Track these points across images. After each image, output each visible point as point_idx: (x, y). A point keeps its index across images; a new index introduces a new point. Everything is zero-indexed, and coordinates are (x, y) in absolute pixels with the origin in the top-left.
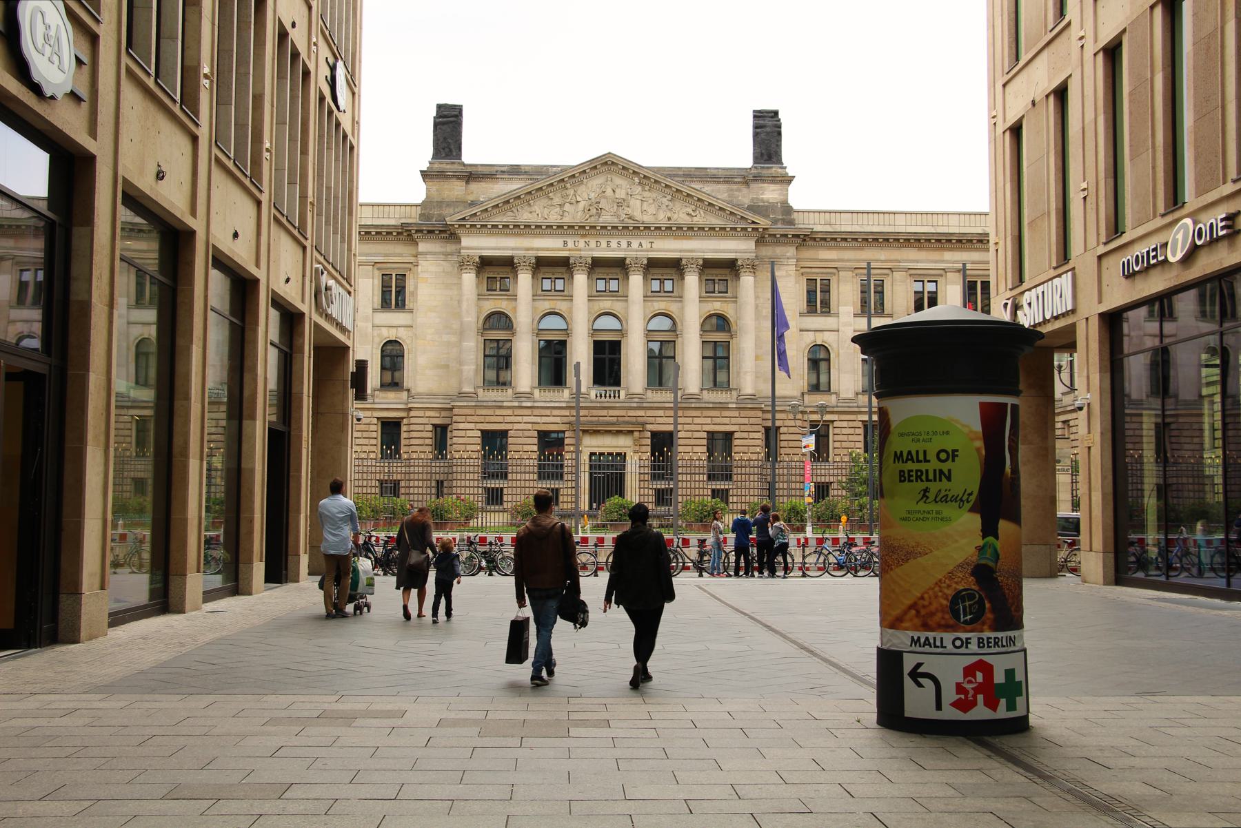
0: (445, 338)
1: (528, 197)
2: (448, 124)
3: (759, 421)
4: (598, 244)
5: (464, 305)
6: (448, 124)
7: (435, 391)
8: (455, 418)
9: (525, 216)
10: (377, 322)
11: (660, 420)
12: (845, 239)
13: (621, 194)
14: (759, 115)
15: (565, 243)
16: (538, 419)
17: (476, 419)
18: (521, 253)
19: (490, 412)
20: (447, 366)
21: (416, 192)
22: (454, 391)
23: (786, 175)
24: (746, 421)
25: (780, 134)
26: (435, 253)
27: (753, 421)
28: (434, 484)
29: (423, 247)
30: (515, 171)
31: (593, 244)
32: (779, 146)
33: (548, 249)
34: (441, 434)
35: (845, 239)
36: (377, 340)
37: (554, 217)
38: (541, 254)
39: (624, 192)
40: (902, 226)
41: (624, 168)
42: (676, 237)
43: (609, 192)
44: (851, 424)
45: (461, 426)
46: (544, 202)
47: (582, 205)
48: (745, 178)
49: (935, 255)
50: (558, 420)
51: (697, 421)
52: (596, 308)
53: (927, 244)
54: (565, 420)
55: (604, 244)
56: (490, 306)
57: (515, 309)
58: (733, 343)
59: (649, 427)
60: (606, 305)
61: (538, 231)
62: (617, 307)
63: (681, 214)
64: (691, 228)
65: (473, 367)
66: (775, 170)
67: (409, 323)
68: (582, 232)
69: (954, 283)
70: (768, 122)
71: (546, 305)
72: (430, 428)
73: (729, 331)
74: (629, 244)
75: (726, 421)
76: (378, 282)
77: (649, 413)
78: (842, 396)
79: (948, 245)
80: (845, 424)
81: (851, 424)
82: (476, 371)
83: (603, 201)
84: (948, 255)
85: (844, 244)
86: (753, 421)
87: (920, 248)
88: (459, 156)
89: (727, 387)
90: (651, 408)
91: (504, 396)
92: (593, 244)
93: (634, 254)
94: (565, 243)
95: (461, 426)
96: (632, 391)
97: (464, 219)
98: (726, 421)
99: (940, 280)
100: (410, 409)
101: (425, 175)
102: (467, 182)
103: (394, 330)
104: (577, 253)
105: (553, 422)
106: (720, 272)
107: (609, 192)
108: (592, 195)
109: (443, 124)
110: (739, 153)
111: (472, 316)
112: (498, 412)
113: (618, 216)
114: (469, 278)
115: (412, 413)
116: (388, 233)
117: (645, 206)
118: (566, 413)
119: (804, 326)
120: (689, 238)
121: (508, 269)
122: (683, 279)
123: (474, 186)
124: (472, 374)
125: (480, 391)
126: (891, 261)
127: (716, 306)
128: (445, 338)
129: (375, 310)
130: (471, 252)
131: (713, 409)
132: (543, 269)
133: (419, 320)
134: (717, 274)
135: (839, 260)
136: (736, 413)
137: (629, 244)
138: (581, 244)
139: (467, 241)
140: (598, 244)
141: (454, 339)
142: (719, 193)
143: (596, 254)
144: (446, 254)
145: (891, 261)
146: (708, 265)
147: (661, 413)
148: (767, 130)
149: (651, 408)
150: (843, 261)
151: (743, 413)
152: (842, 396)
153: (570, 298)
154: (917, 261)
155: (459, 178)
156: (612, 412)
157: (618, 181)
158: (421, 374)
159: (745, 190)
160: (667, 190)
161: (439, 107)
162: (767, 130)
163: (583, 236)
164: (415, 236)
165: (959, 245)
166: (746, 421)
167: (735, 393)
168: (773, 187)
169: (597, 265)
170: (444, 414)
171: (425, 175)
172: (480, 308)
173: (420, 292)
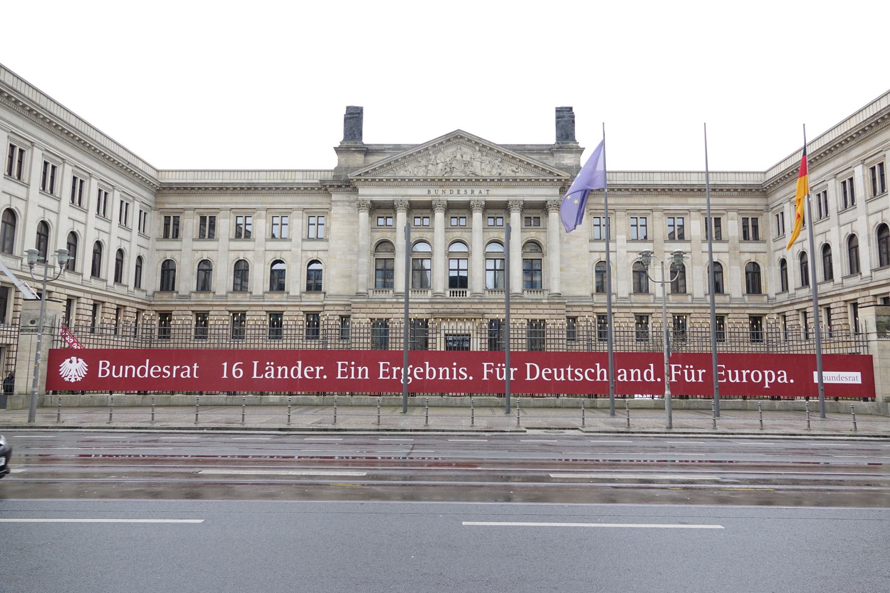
0: (349, 257)
1: (404, 160)
2: (354, 119)
3: (564, 312)
5: (360, 235)
6: (354, 119)
7: (341, 293)
8: (353, 310)
9: (401, 173)
10: (305, 248)
11: (494, 311)
12: (620, 190)
13: (467, 158)
14: (559, 110)
15: (429, 191)
17: (367, 311)
19: (377, 306)
20: (350, 276)
21: (330, 162)
23: (578, 147)
24: (554, 312)
25: (573, 122)
26: (343, 201)
27: (559, 312)
29: (335, 197)
30: (397, 148)
31: (448, 191)
32: (573, 130)
34: (344, 319)
35: (620, 190)
36: (304, 260)
37: (421, 173)
38: (413, 199)
39: (469, 157)
40: (658, 180)
41: (469, 140)
42: (506, 187)
43: (459, 157)
44: (627, 315)
45: (357, 316)
46: (415, 164)
47: (440, 166)
48: (550, 151)
49: (682, 200)
50: (423, 311)
51: (520, 311)
52: (451, 237)
53: (677, 193)
54: (429, 311)
55: (455, 192)
56: (379, 236)
58: (544, 260)
59: (486, 316)
60: (457, 235)
61: (411, 183)
62: (465, 236)
63: (508, 171)
64: (515, 180)
66: (571, 144)
67: (326, 248)
68: (440, 183)
69: (695, 219)
70: (565, 114)
71: (415, 236)
72: (337, 318)
73: (541, 252)
74: (473, 192)
75: (541, 311)
77: (487, 306)
78: (619, 296)
79: (692, 193)
80: (622, 315)
81: (627, 315)
82: (369, 280)
83: (454, 162)
84: (691, 200)
85: (619, 193)
86: (559, 312)
87: (672, 196)
88: (361, 138)
89: (541, 291)
90: (488, 303)
91: (388, 296)
94: (429, 191)
95: (357, 316)
96: (475, 291)
98: (541, 311)
99: (686, 218)
100: (325, 305)
101: (337, 150)
102: (365, 156)
103: (316, 253)
106: (536, 212)
107: (459, 157)
108: (448, 159)
109: (350, 118)
110: (546, 134)
112: (382, 306)
113: (465, 172)
114: (364, 216)
115: (326, 308)
116: (312, 189)
117: (483, 166)
118: (429, 306)
119: (592, 249)
121: (391, 211)
122: (509, 216)
124: (365, 280)
125: (371, 292)
126: (652, 205)
127: (532, 235)
128: (349, 257)
129: (303, 240)
131: (532, 303)
132: (415, 211)
134: (533, 213)
135: (615, 204)
136: (547, 307)
137: (473, 192)
139: (361, 191)
141: (354, 258)
142: (534, 159)
143: (450, 199)
145: (652, 205)
146: (526, 207)
147: (495, 306)
148: (565, 120)
149: (488, 303)
150: (618, 204)
151: (552, 306)
152: (619, 296)
153: (432, 230)
154: (670, 205)
155: (359, 152)
156: (461, 306)
157: (465, 149)
159: (551, 159)
160: (498, 155)
161: (348, 108)
162: (565, 120)
163: (441, 186)
164: (329, 190)
165: (699, 193)
166: (554, 312)
167: (546, 292)
168: (570, 155)
169: (450, 208)
170: (347, 308)
171: (337, 150)
172: (372, 237)
173: (332, 227)
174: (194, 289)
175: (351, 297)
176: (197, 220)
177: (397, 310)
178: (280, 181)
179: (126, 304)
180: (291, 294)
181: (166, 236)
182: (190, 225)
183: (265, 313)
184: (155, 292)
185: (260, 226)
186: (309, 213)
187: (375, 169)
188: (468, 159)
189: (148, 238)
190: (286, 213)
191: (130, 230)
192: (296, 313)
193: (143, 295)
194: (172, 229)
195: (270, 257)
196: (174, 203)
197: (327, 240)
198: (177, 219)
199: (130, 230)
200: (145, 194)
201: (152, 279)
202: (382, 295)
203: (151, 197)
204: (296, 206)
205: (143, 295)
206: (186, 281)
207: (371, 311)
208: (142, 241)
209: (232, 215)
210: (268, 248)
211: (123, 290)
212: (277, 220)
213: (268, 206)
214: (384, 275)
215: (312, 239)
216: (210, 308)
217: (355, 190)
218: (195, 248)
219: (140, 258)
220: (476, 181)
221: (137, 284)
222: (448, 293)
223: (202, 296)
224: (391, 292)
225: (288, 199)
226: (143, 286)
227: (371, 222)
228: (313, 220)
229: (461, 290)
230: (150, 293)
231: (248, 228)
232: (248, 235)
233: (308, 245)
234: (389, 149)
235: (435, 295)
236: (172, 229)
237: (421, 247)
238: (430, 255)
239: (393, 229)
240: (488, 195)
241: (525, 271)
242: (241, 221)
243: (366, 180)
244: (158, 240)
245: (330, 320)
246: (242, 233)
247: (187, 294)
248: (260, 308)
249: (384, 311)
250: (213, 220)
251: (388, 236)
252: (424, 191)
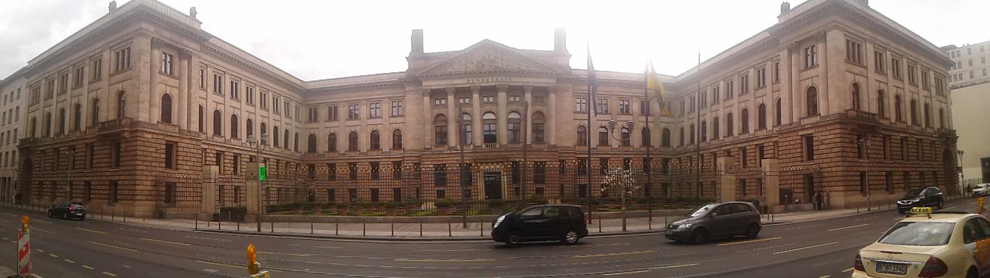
2: (417, 39)
4: (483, 80)
6: (417, 39)
7: (415, 149)
8: (423, 160)
10: (391, 122)
15: (468, 81)
19: (437, 156)
21: (403, 67)
22: (422, 148)
28: (415, 189)
31: (481, 80)
55: (486, 80)
56: (436, 112)
57: (447, 113)
59: (511, 160)
60: (488, 108)
62: (493, 108)
65: (430, 138)
75: (543, 156)
82: (431, 140)
89: (544, 143)
91: (444, 149)
92: (481, 80)
94: (468, 81)
98: (543, 156)
111: (428, 116)
114: (427, 99)
115: (405, 159)
118: (472, 155)
125: (433, 147)
130: (427, 88)
133: (407, 119)
137: (497, 79)
138: (476, 81)
139: (424, 84)
140: (483, 80)
143: (483, 85)
144: (417, 91)
156: (493, 154)
158: (409, 142)
167: (546, 145)
170: (419, 158)
174: (327, 150)
175: (420, 151)
179: (291, 160)
180: (384, 150)
181: (310, 120)
182: (323, 112)
183: (368, 164)
184: (305, 153)
185: (363, 111)
186: (392, 100)
189: (301, 122)
190: (379, 101)
191: (291, 118)
192: (387, 163)
193: (299, 155)
194: (313, 116)
195: (370, 129)
197: (404, 116)
198: (315, 110)
199: (291, 118)
200: (297, 96)
201: (304, 146)
202: (441, 149)
203: (301, 98)
205: (299, 155)
206: (322, 146)
208: (297, 124)
211: (289, 153)
212: (373, 106)
214: (442, 136)
215: (395, 116)
216: (336, 162)
217: (421, 84)
219: (297, 134)
221: (296, 149)
222: (484, 146)
223: (331, 154)
224: (446, 147)
225: (380, 92)
226: (299, 150)
227: (431, 103)
228: (395, 104)
229: (493, 144)
230: (303, 153)
231: (357, 112)
232: (356, 117)
233: (393, 120)
235: (476, 147)
236: (313, 116)
237: (466, 117)
238: (471, 122)
239: (446, 106)
241: (533, 131)
242: (352, 108)
243: (427, 76)
244: (306, 123)
245: (408, 165)
246: (353, 116)
247: (323, 153)
248: (365, 161)
249: (442, 159)
250: (336, 108)
251: (443, 111)
252: (465, 81)
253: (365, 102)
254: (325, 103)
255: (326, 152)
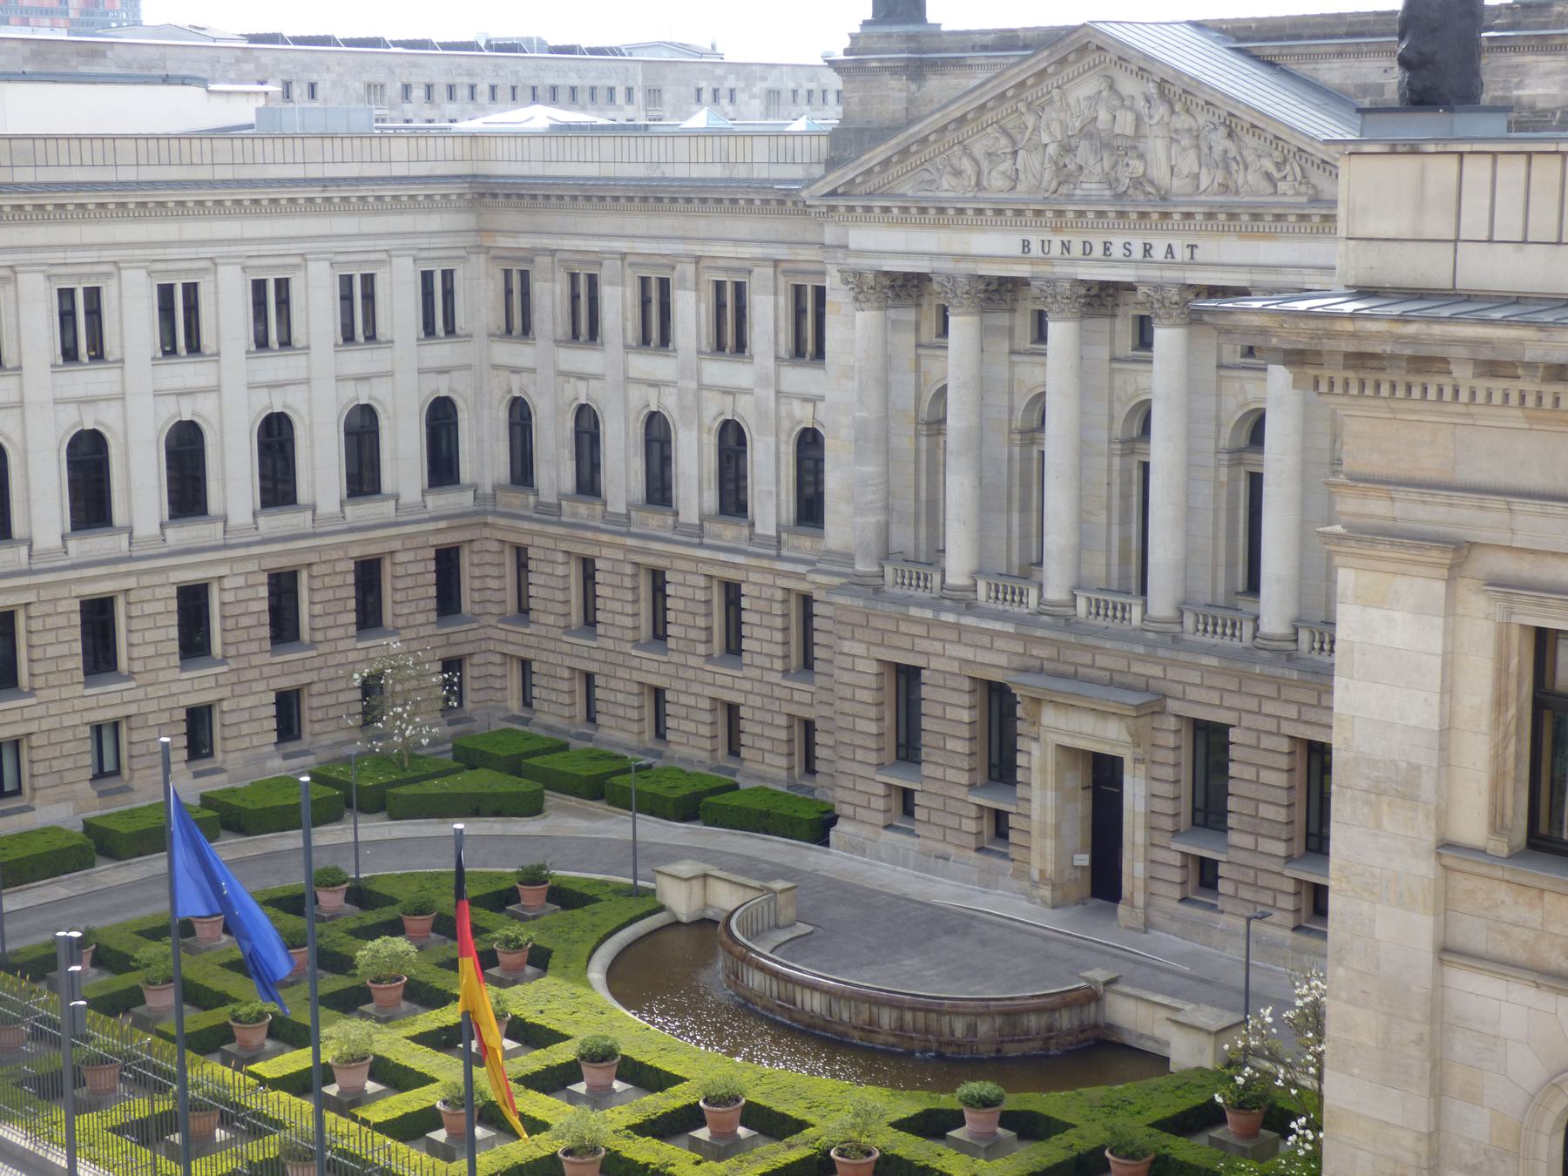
4: (1087, 248)
13: (1125, 123)
15: (1026, 245)
16: (969, 654)
18: (947, 266)
33: (991, 258)
36: (786, 425)
42: (1244, 234)
43: (1103, 115)
50: (1002, 660)
51: (1269, 707)
52: (1131, 389)
55: (1098, 251)
74: (1147, 250)
76: (785, 301)
92: (1077, 250)
93: (1153, 274)
94: (1026, 245)
97: (833, 193)
104: (1044, 269)
105: (996, 663)
112: (904, 627)
120: (1270, 236)
123: (935, 85)
137: (1147, 250)
138: (1056, 249)
147: (1194, 677)
155: (894, 71)
163: (1056, 230)
168: (1547, 62)
176: (561, 288)
177: (938, 646)
178: (716, 172)
179: (397, 545)
184: (496, 488)
187: (870, 171)
188: (1130, 131)
192: (767, 593)
196: (519, 233)
200: (435, 222)
204: (757, 251)
207: (876, 637)
209: (628, 272)
210: (706, 380)
213: (698, 249)
218: (563, 367)
220: (1147, 206)
225: (742, 226)
234: (985, 48)
240: (1192, 263)
253: (690, 269)
254: (553, 252)
255: (568, 497)
